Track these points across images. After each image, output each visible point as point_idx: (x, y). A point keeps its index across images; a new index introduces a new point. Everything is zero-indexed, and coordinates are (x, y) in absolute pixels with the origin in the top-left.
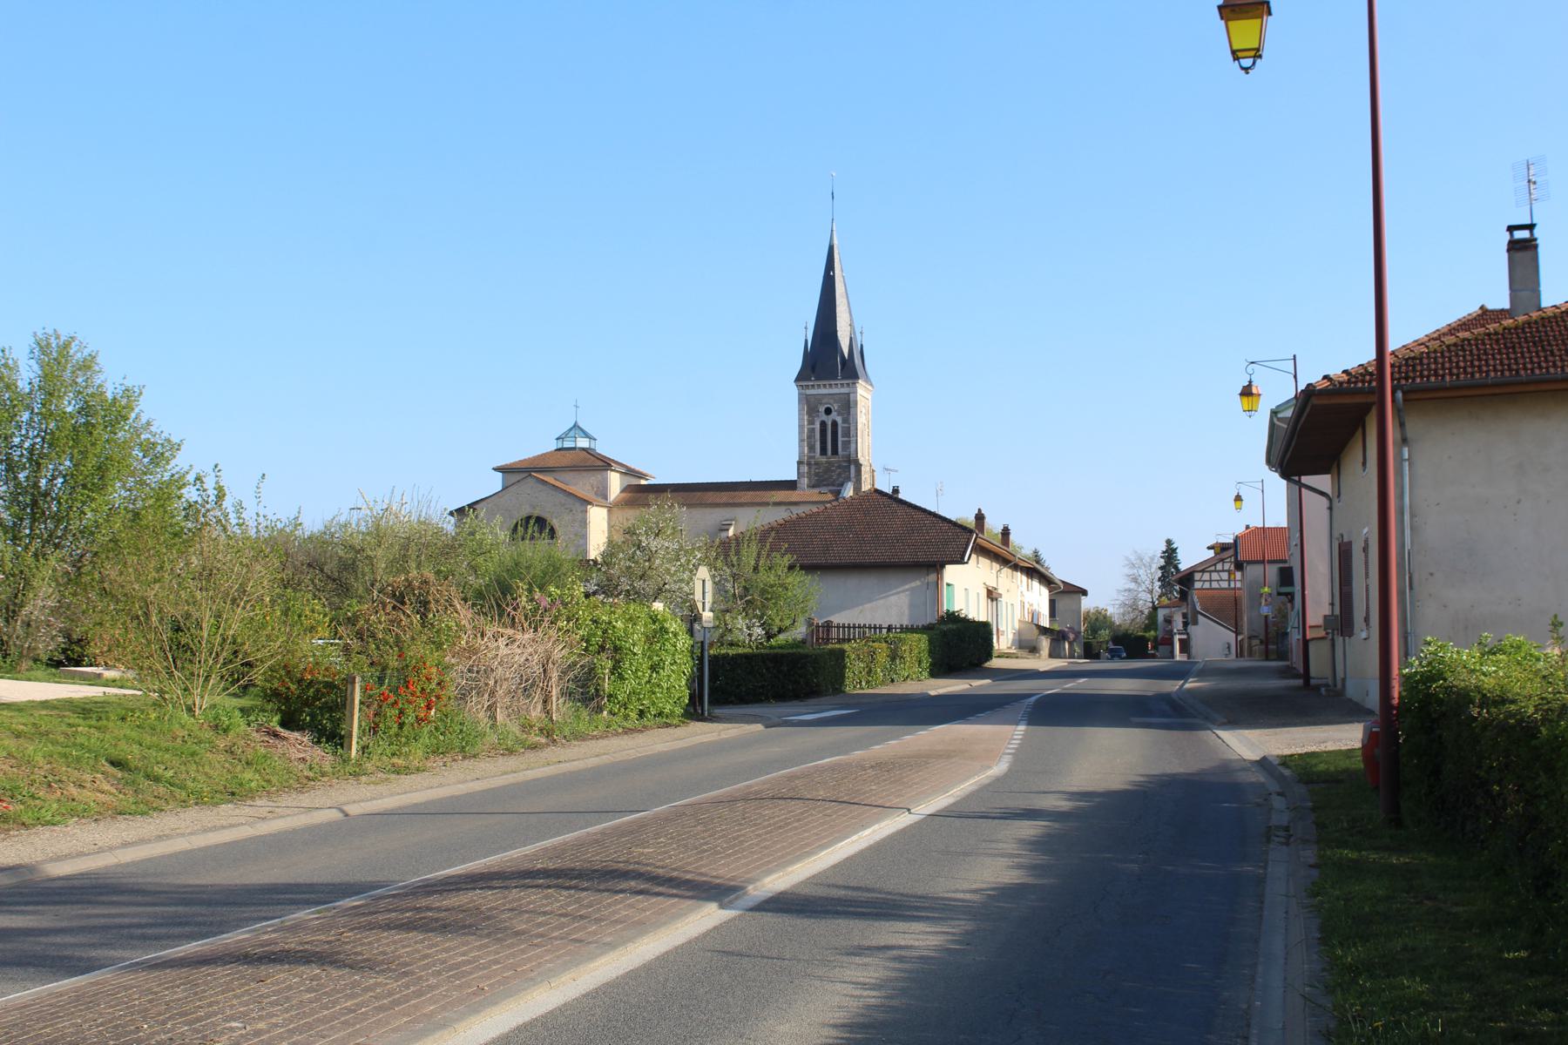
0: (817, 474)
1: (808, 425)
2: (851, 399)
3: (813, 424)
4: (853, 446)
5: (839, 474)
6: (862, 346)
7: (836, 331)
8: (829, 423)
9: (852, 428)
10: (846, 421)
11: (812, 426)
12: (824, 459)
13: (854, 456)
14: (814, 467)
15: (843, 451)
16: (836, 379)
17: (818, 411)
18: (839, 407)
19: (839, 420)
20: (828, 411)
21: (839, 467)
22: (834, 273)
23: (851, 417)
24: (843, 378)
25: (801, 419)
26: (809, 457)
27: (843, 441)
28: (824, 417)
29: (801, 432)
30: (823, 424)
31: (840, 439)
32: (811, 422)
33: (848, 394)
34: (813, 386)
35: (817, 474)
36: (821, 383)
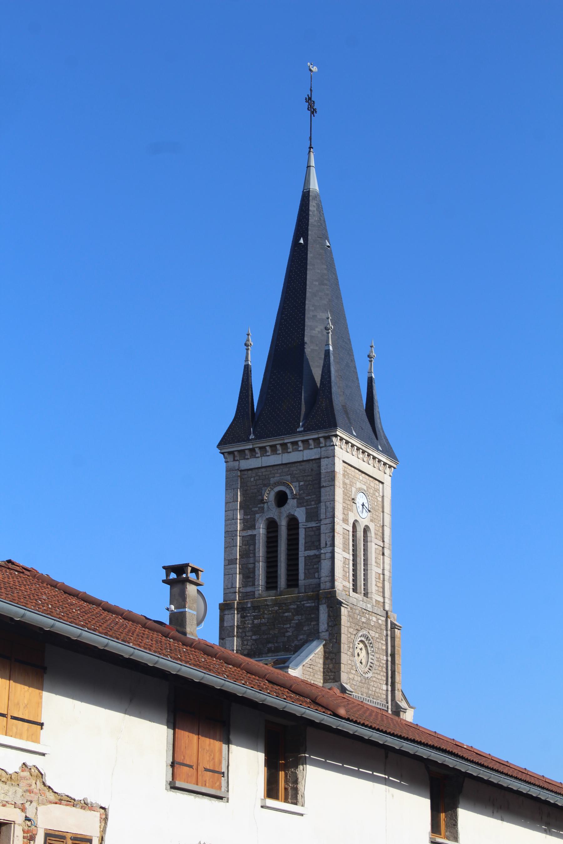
0: (256, 629)
1: (243, 530)
2: (323, 471)
3: (253, 527)
4: (325, 564)
5: (299, 627)
6: (370, 381)
7: (302, 345)
8: (283, 524)
9: (323, 528)
10: (313, 515)
11: (250, 532)
12: (270, 597)
13: (328, 585)
14: (250, 614)
15: (306, 577)
16: (292, 431)
17: (262, 501)
18: (301, 489)
19: (301, 514)
20: (281, 499)
21: (298, 611)
22: (306, 240)
23: (322, 504)
24: (308, 429)
25: (230, 520)
26: (245, 596)
27: (307, 558)
28: (273, 512)
29: (229, 546)
30: (272, 526)
31: (302, 553)
32: (249, 524)
33: (318, 460)
34: (252, 450)
35: (256, 629)
36: (267, 443)
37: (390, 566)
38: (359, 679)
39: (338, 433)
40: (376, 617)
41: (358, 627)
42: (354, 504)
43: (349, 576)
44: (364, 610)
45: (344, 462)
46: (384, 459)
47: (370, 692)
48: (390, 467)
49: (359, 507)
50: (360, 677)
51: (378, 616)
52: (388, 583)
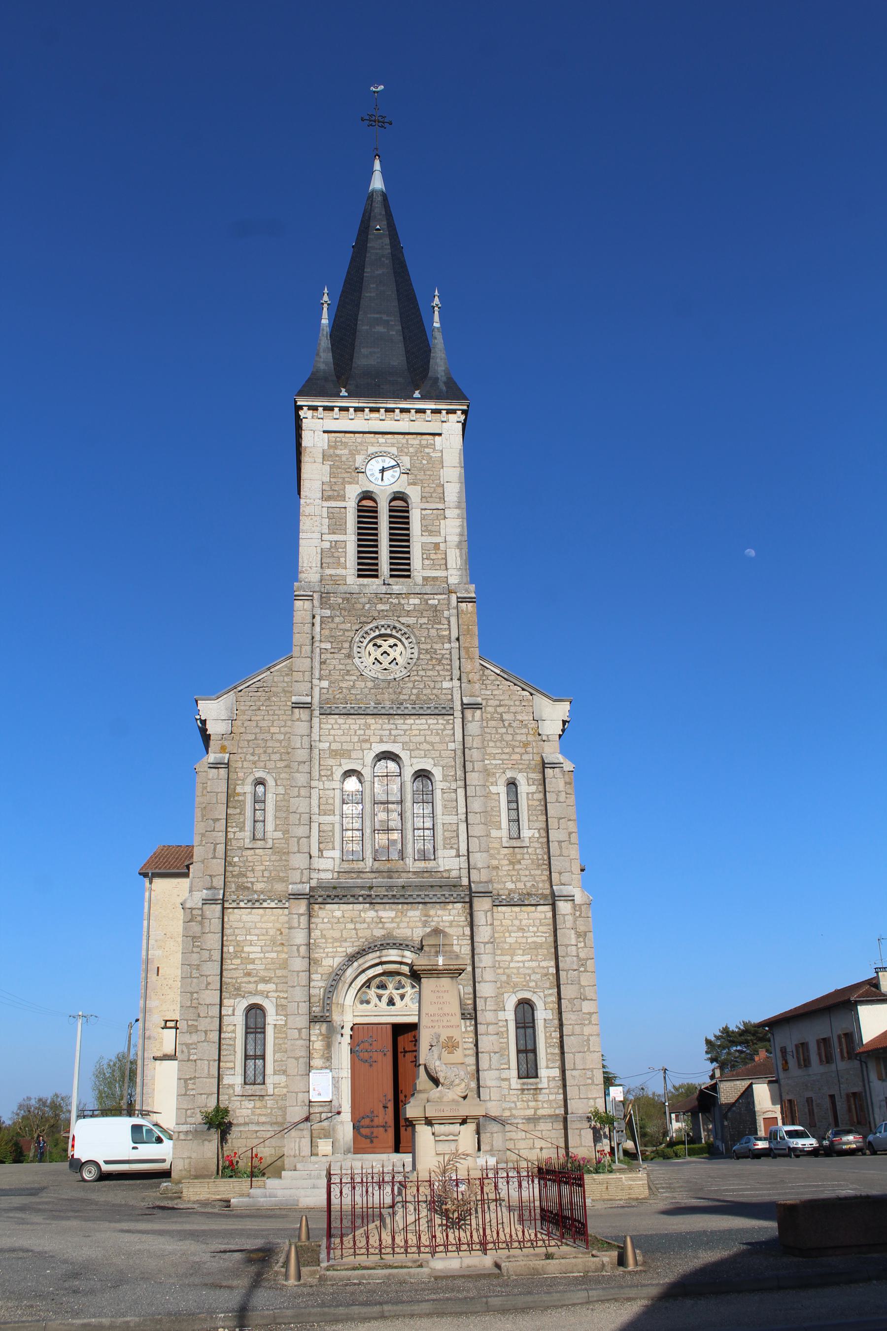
37: (463, 528)
38: (370, 684)
39: (299, 403)
40: (420, 599)
41: (363, 619)
42: (360, 474)
43: (345, 561)
44: (381, 596)
45: (325, 432)
46: (430, 405)
47: (402, 697)
48: (450, 412)
49: (372, 475)
50: (372, 681)
51: (426, 597)
52: (457, 551)
